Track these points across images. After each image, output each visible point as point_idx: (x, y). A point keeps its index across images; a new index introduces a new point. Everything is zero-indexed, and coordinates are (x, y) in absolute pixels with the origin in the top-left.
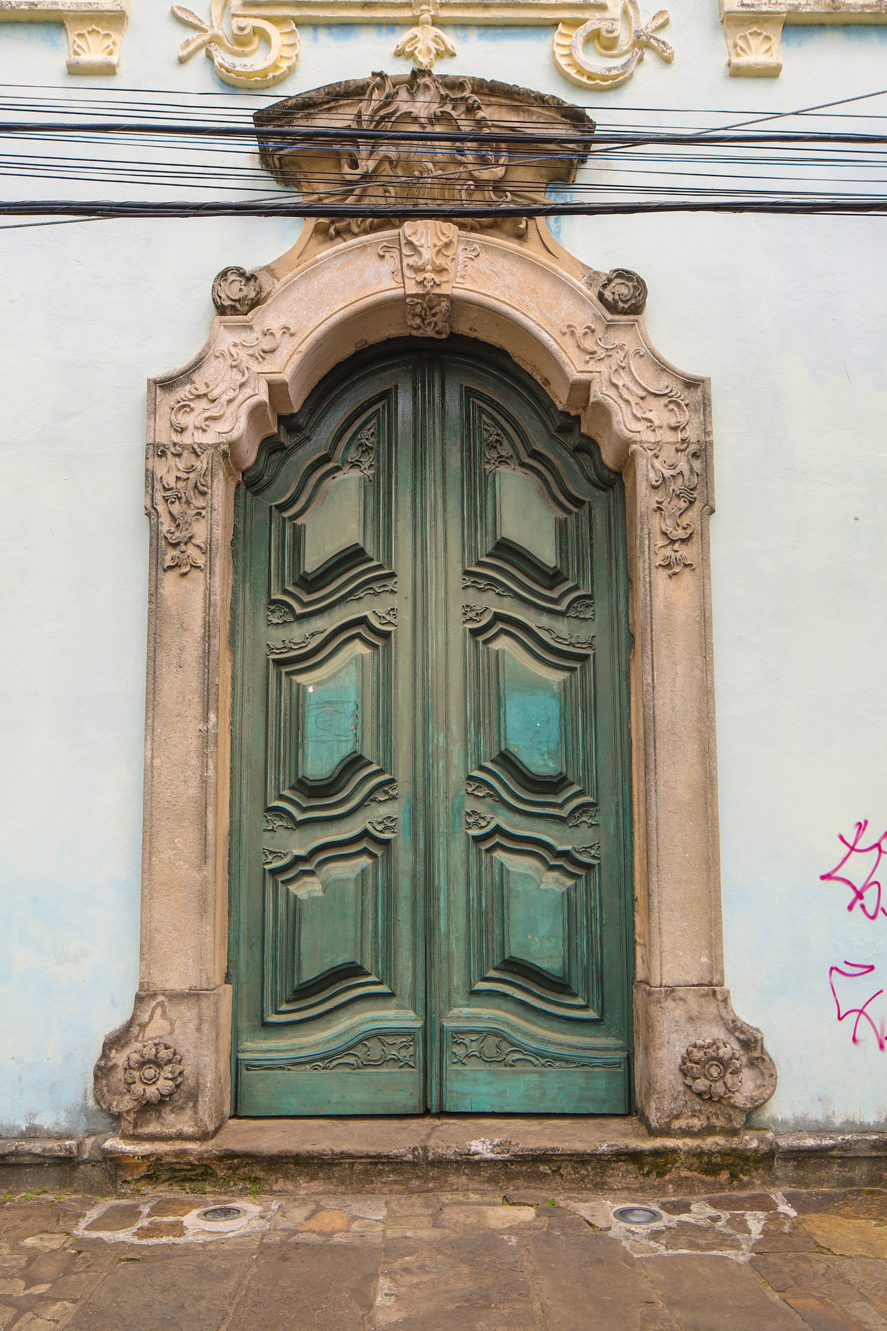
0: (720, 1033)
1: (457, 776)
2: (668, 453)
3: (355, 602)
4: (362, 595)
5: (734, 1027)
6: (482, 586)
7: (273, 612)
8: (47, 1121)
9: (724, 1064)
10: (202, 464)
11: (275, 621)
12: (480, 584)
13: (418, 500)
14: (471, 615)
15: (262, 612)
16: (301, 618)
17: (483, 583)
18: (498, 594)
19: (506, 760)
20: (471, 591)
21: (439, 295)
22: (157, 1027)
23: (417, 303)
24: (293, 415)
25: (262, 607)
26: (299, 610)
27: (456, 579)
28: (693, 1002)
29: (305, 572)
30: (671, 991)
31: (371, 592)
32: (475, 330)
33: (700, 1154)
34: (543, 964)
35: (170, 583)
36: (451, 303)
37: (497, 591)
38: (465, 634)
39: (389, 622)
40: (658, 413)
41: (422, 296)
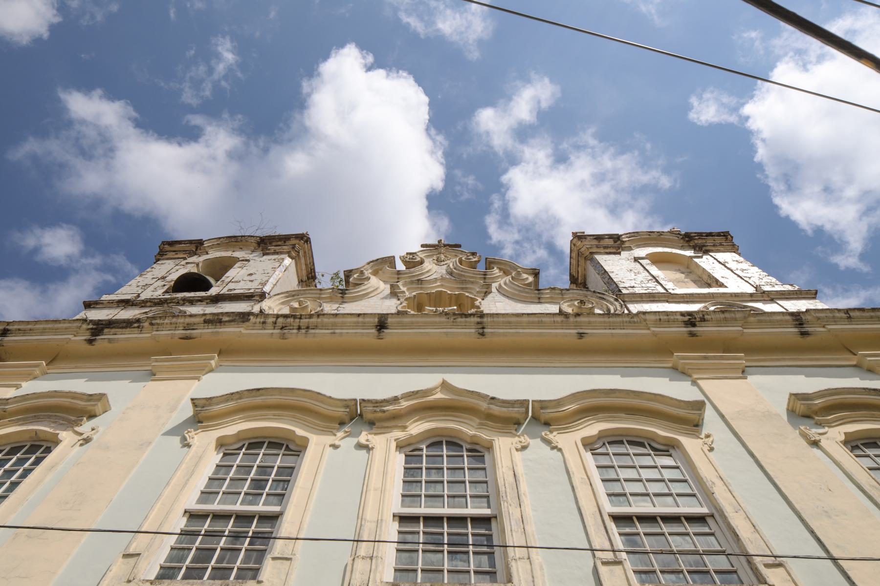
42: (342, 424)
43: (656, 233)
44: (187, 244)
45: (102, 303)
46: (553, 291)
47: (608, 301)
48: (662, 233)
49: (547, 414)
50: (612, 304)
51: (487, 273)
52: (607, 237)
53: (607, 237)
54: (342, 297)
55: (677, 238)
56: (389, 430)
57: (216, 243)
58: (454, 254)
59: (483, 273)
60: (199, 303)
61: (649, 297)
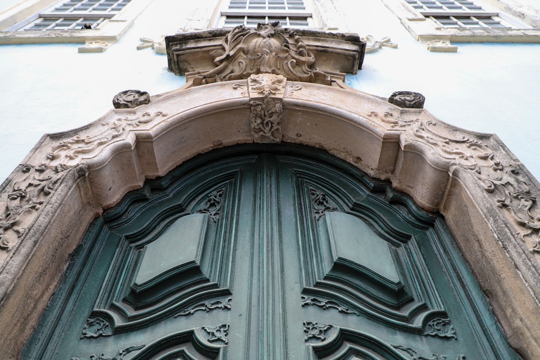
3: (183, 318)
4: (192, 311)
6: (322, 304)
7: (91, 325)
11: (89, 334)
12: (320, 302)
13: (256, 234)
14: (316, 332)
15: (80, 325)
16: (120, 332)
17: (323, 302)
18: (341, 312)
20: (311, 310)
21: (274, 99)
23: (258, 105)
24: (159, 178)
25: (82, 320)
26: (118, 322)
29: (135, 284)
31: (203, 308)
32: (301, 135)
36: (283, 106)
37: (340, 309)
38: (309, 353)
39: (219, 340)
41: (262, 99)
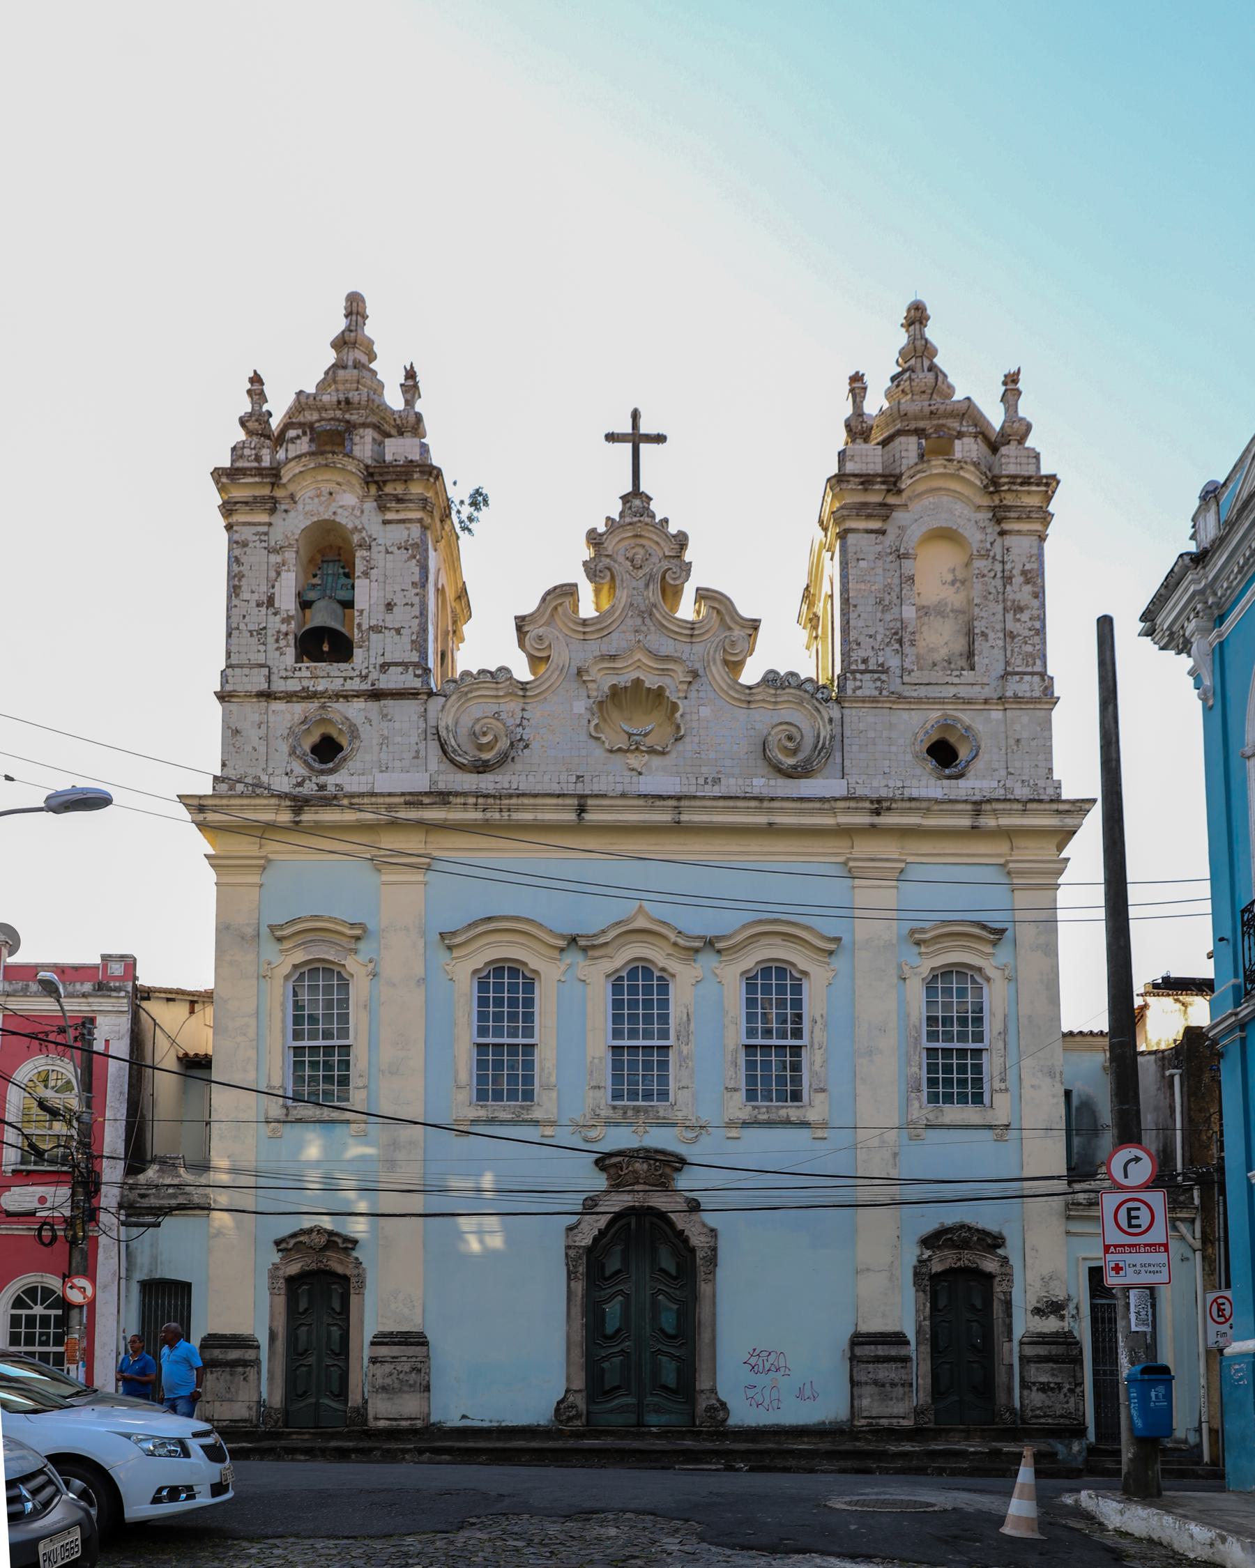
0: (714, 1402)
1: (648, 1334)
2: (706, 1249)
5: (718, 1400)
8: (542, 1423)
9: (715, 1409)
10: (581, 1251)
19: (662, 1330)
22: (571, 1399)
27: (648, 1278)
28: (708, 1394)
30: (702, 1391)
33: (709, 1432)
34: (671, 1386)
35: (573, 1284)
40: (703, 1239)
42: (562, 950)
43: (955, 463)
44: (255, 475)
45: (238, 696)
46: (767, 690)
47: (822, 718)
48: (964, 466)
49: (719, 945)
50: (824, 726)
51: (696, 626)
52: (879, 479)
53: (879, 479)
54: (524, 696)
55: (979, 483)
56: (600, 961)
57: (297, 471)
58: (655, 538)
59: (689, 626)
60: (355, 699)
61: (873, 702)
